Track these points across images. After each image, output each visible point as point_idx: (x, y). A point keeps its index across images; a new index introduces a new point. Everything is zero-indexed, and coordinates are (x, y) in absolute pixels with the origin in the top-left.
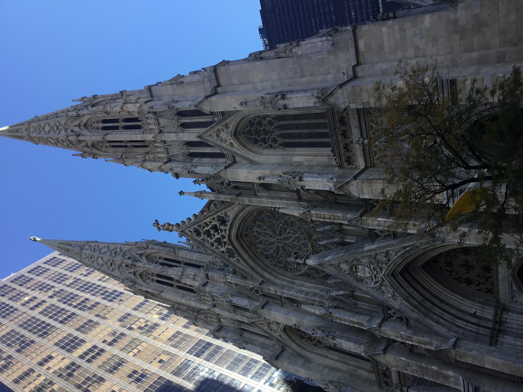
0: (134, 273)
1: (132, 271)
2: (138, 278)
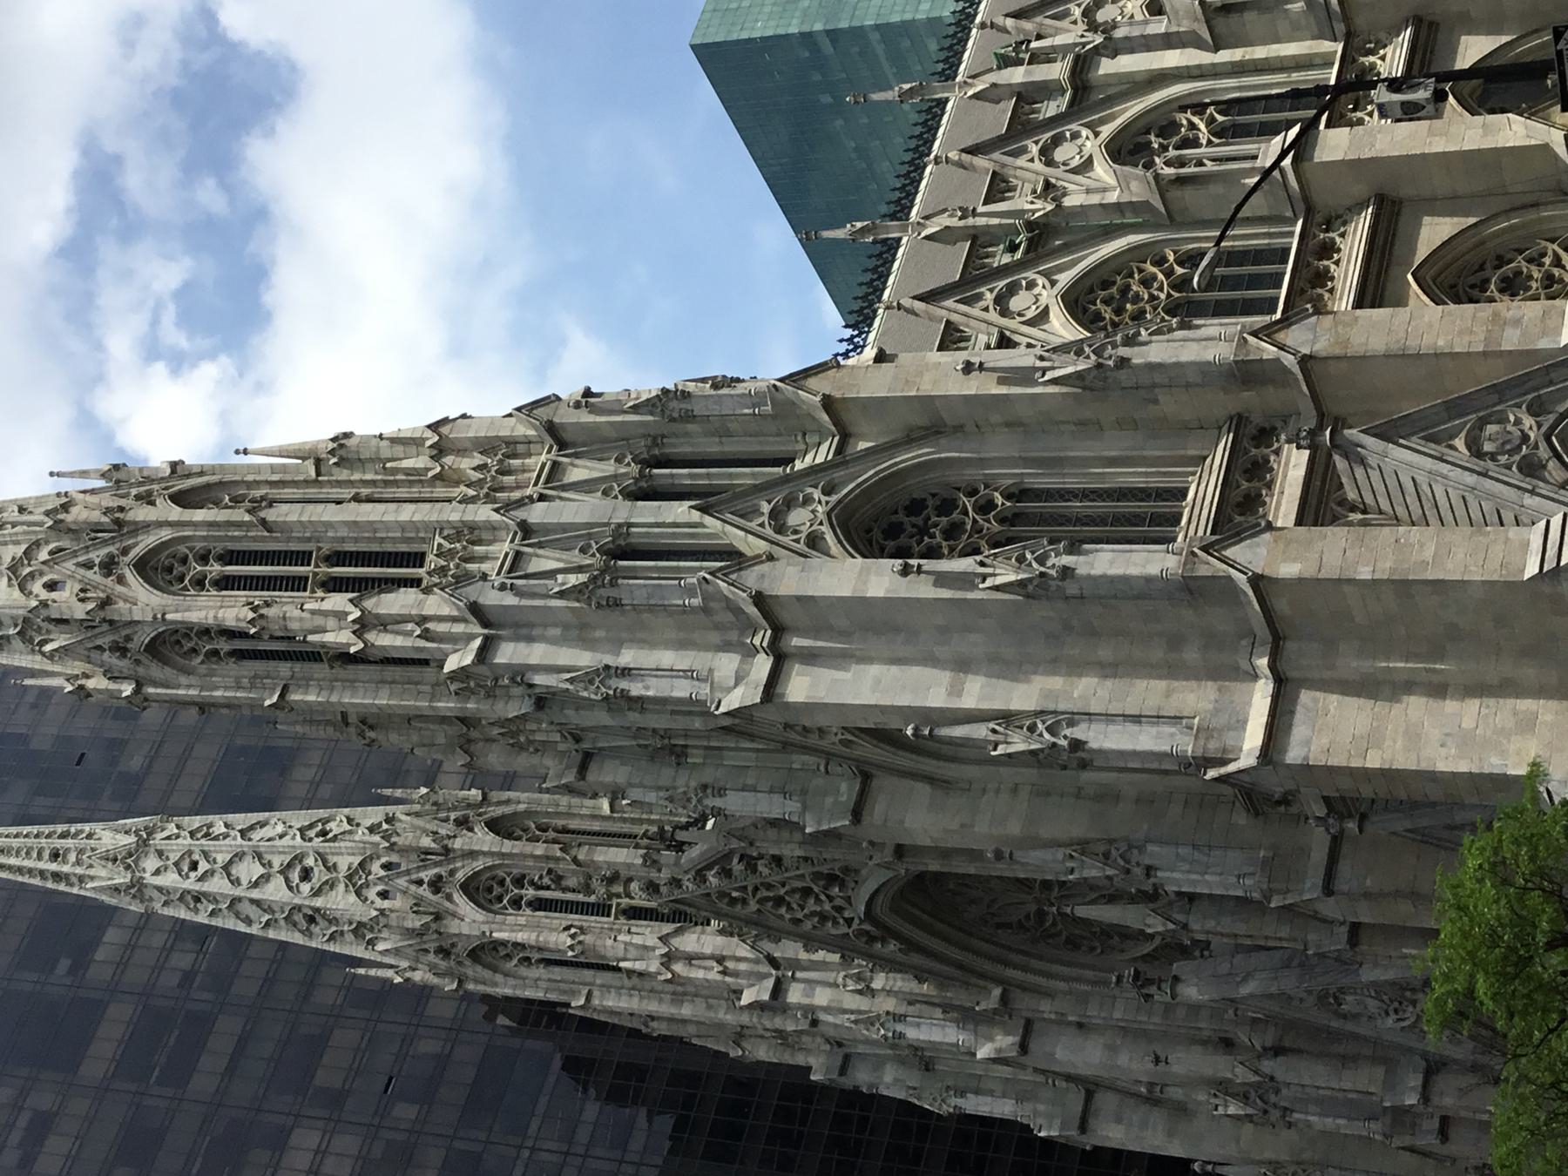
0: (444, 952)
1: (432, 946)
2: (468, 962)
